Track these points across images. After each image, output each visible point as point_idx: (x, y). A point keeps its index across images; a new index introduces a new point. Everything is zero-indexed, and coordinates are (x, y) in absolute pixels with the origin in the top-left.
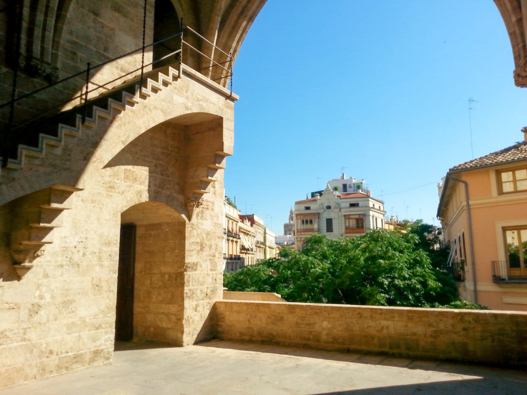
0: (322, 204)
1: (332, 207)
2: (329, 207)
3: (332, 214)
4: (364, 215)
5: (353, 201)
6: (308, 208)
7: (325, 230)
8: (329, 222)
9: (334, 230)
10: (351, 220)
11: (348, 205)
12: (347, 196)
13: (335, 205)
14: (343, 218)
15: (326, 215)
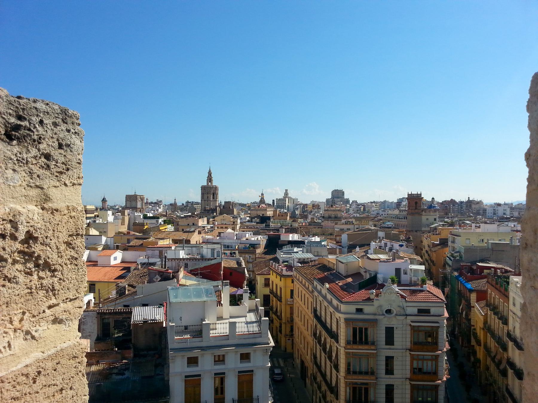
0: (380, 306)
1: (395, 312)
2: (389, 311)
3: (393, 322)
4: (439, 327)
5: (424, 306)
6: (359, 311)
7: (384, 343)
8: (390, 332)
9: (395, 343)
10: (421, 333)
11: (415, 311)
12: (414, 298)
13: (399, 309)
14: (409, 328)
15: (385, 322)
